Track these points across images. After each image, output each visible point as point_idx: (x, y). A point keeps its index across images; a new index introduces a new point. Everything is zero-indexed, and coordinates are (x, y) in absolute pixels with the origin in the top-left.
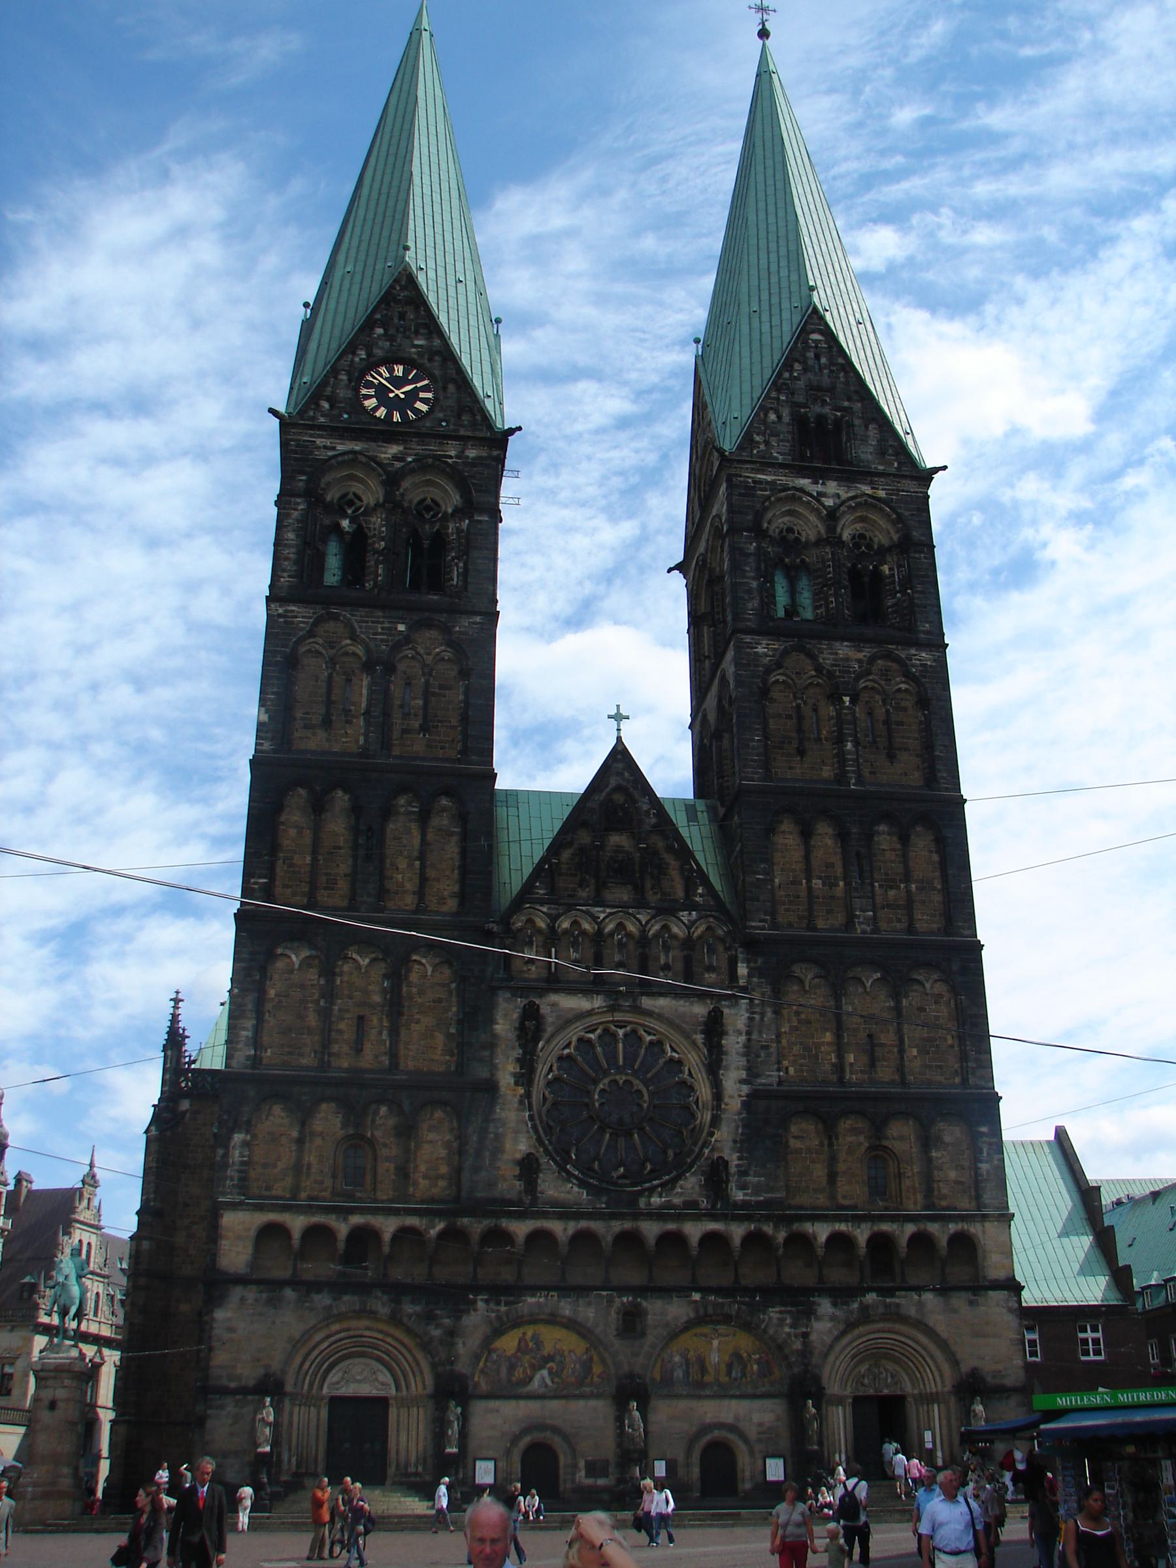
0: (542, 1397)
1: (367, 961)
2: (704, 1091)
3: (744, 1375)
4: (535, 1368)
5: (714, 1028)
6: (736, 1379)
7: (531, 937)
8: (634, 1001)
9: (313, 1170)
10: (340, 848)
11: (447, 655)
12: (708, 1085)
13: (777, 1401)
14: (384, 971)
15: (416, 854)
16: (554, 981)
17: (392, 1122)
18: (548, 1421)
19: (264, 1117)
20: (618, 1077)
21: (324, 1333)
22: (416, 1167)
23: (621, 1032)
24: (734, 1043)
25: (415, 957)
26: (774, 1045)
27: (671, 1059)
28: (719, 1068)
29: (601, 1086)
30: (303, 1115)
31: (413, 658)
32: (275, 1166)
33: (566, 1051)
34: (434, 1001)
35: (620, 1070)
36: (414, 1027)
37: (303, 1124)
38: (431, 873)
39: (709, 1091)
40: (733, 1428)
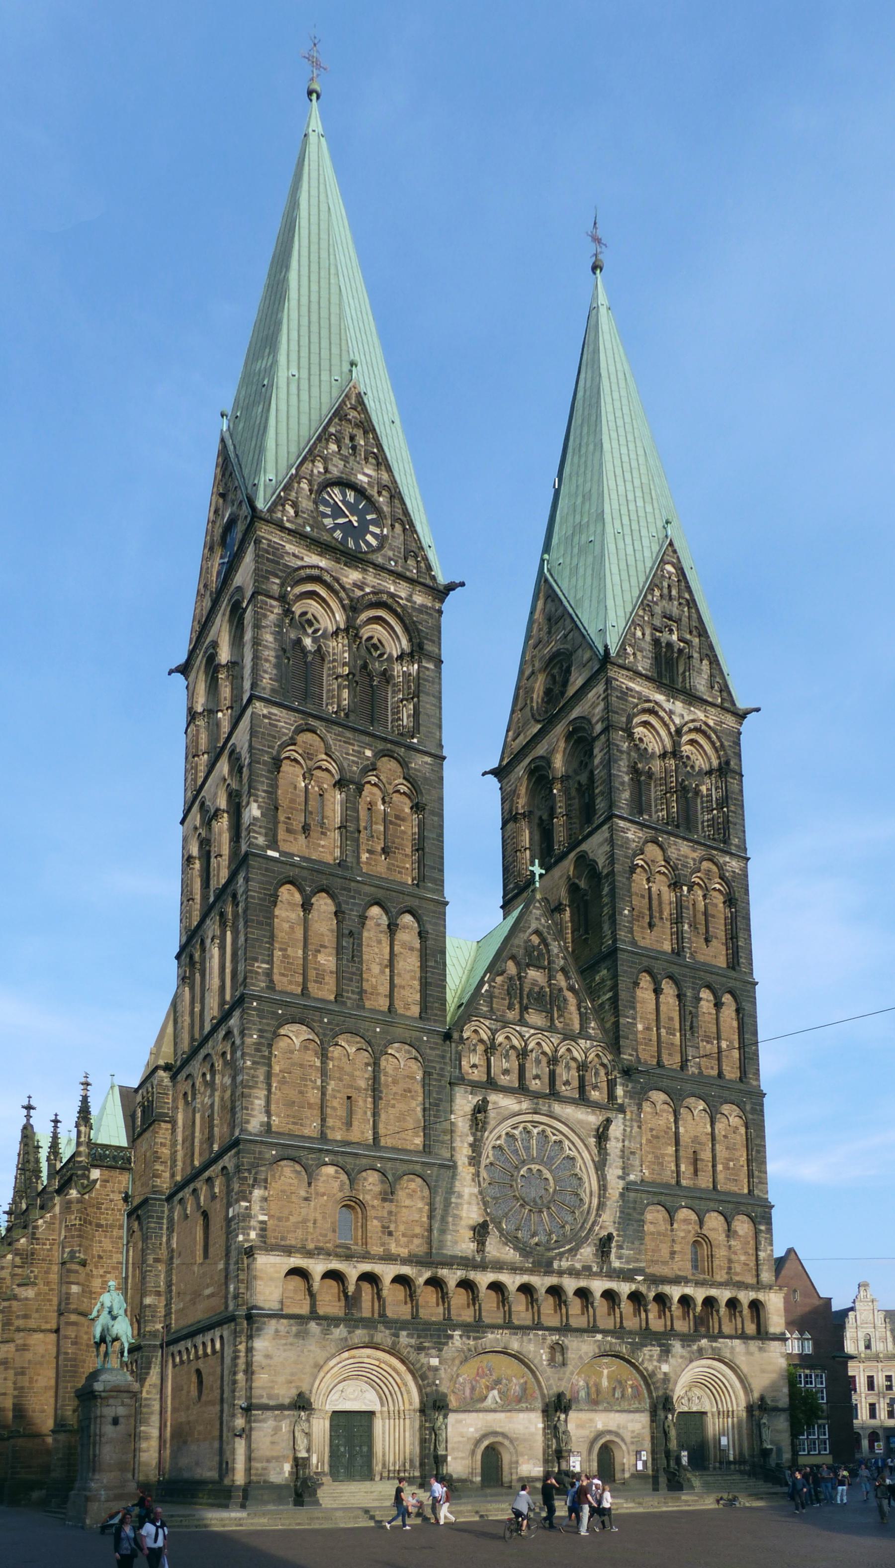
0: (494, 1411)
1: (354, 1049)
2: (591, 1182)
3: (623, 1396)
4: (490, 1388)
5: (602, 1136)
6: (618, 1399)
7: (475, 1045)
8: (550, 1106)
9: (318, 1225)
10: (325, 947)
11: (403, 789)
12: (595, 1178)
13: (642, 1414)
14: (366, 1061)
15: (386, 962)
16: (491, 1084)
17: (377, 1189)
18: (498, 1430)
19: (277, 1175)
20: (533, 1166)
21: (337, 1359)
22: (397, 1227)
23: (535, 1131)
24: (614, 1146)
25: (390, 1051)
26: (638, 1152)
27: (568, 1157)
28: (605, 1166)
29: (522, 1173)
30: (310, 1178)
31: (375, 785)
32: (288, 1219)
33: (498, 1142)
34: (405, 1091)
35: (533, 1160)
36: (391, 1111)
37: (310, 1184)
38: (397, 981)
39: (596, 1183)
40: (617, 1434)
